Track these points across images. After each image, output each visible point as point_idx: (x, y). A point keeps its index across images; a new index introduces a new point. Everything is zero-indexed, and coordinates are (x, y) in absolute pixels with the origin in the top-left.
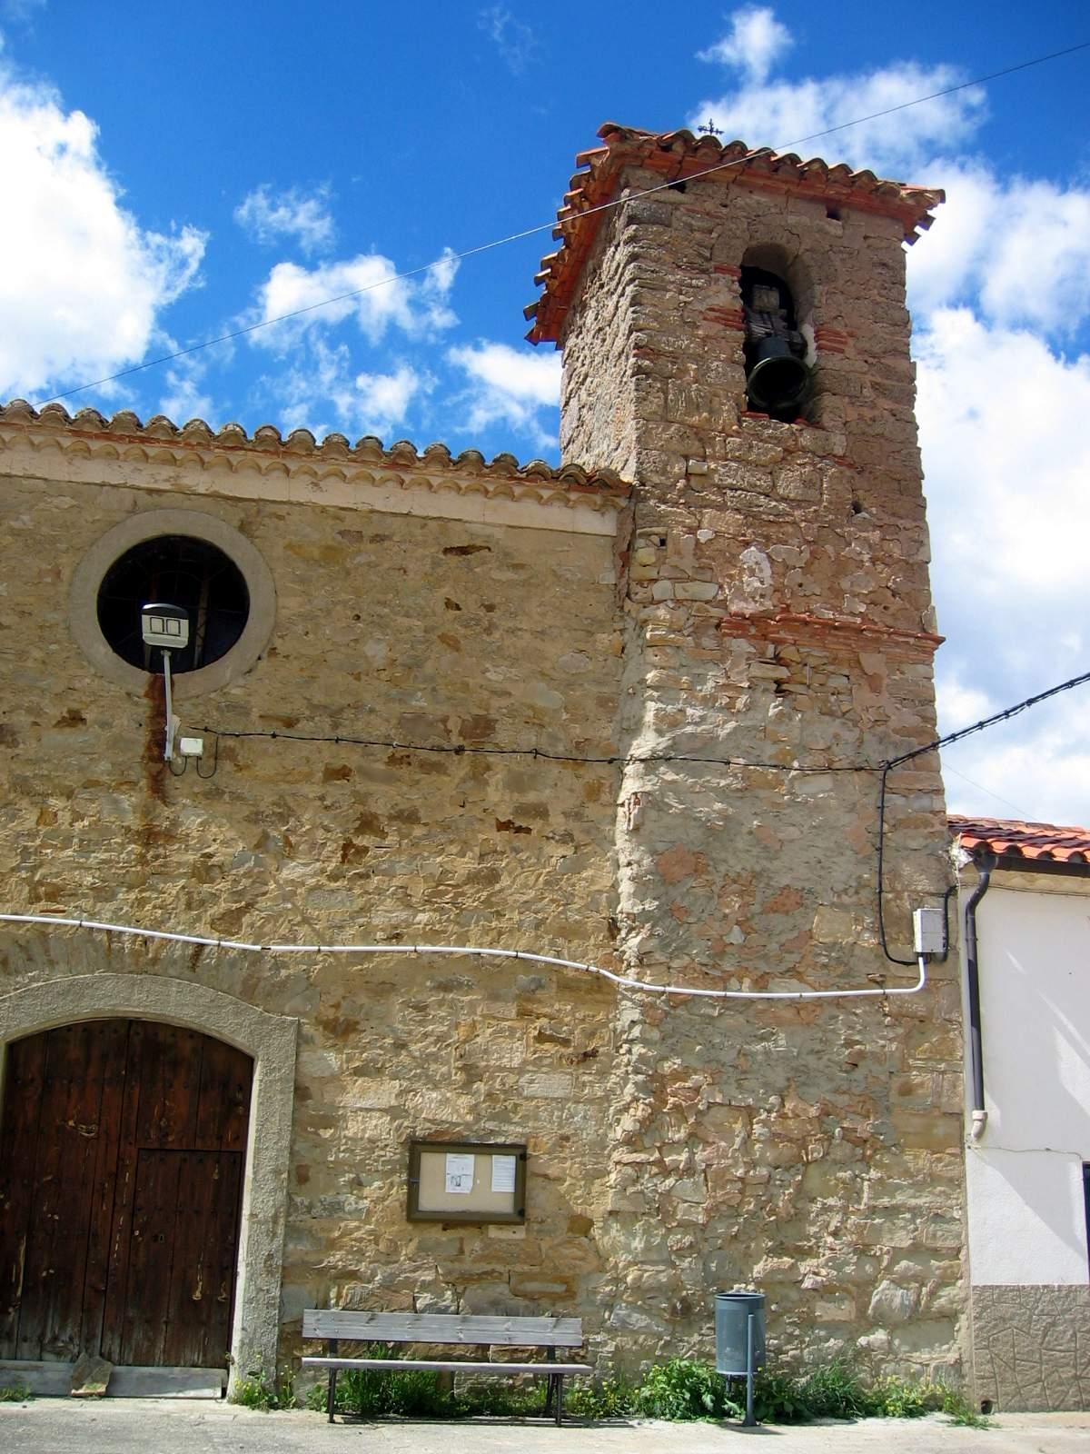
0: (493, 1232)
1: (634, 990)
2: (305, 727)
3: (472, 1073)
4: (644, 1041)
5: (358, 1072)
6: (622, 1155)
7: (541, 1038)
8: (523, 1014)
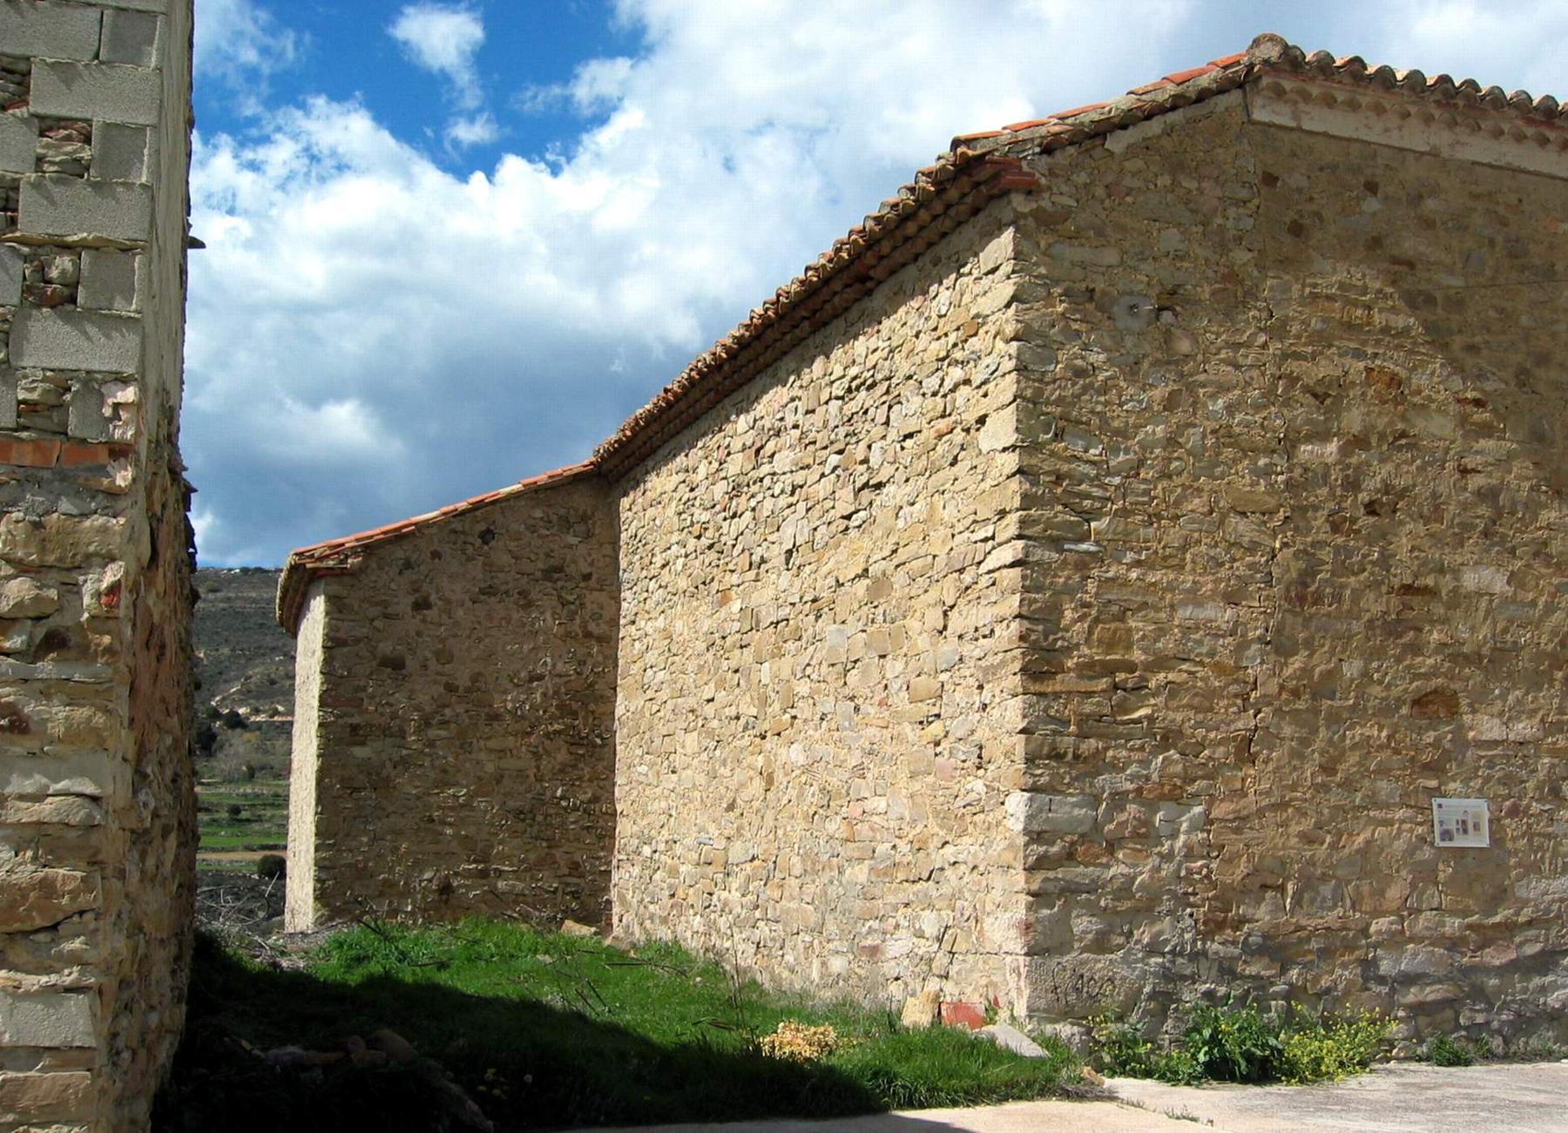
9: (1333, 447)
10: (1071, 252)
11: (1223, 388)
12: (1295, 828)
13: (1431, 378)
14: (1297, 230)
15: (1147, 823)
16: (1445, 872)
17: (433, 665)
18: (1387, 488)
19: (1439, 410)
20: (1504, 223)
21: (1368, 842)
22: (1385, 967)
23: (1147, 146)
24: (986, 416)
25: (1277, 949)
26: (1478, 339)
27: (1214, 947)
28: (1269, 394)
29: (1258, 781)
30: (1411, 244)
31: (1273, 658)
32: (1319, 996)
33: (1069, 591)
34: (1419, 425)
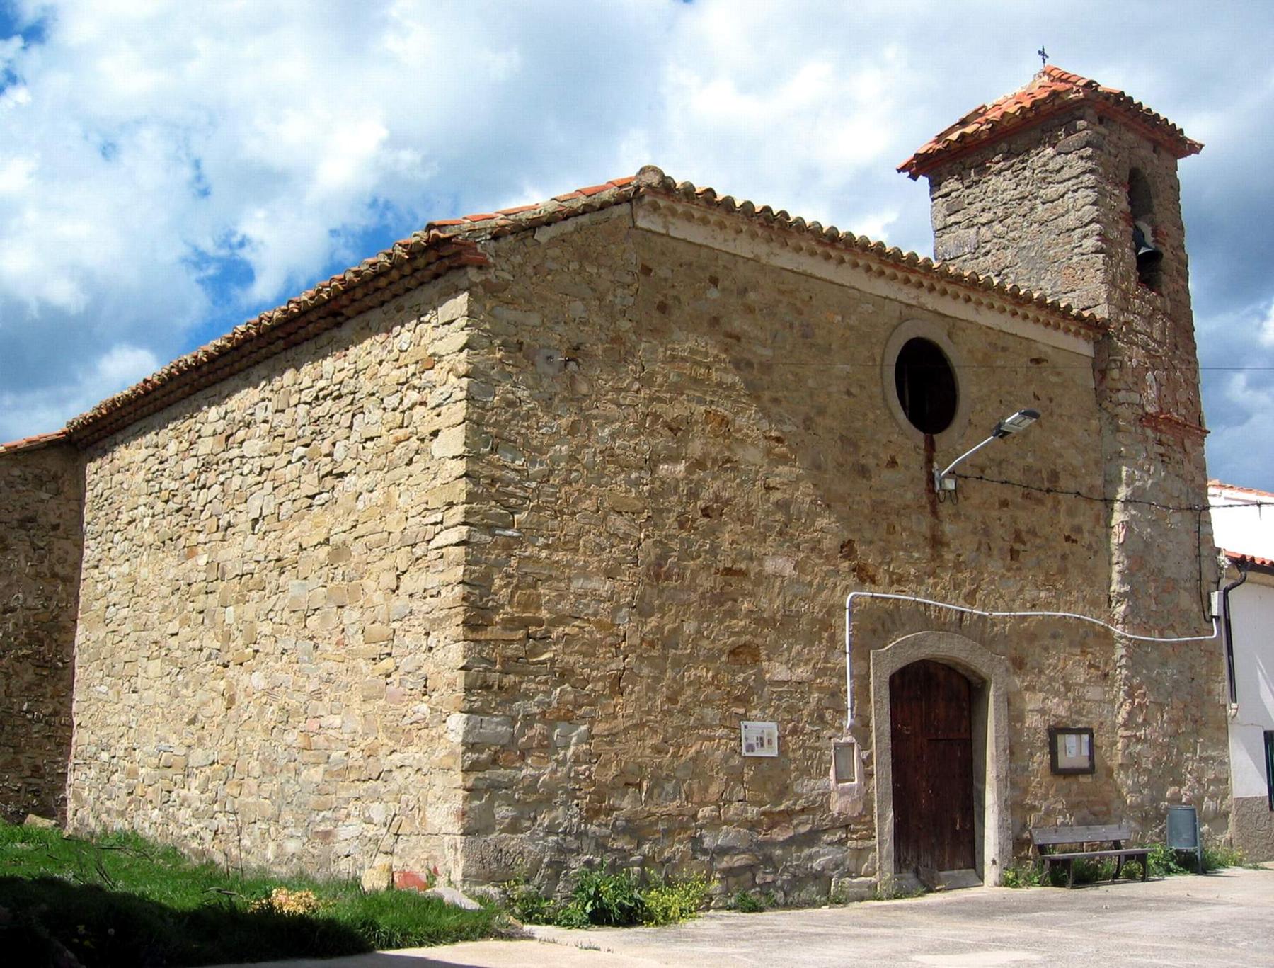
0: (1082, 779)
1: (1121, 637)
3: (1068, 686)
4: (1125, 666)
5: (1027, 688)
6: (1121, 732)
7: (1090, 666)
8: (1083, 652)
9: (681, 467)
10: (510, 314)
11: (608, 421)
12: (649, 742)
13: (748, 421)
14: (663, 308)
15: (548, 737)
16: (748, 774)
18: (717, 498)
19: (752, 443)
21: (698, 752)
22: (708, 842)
23: (563, 240)
24: (439, 430)
25: (635, 830)
26: (780, 394)
27: (592, 828)
28: (640, 427)
29: (625, 708)
30: (739, 324)
31: (636, 618)
32: (663, 863)
33: (498, 565)
34: (739, 454)
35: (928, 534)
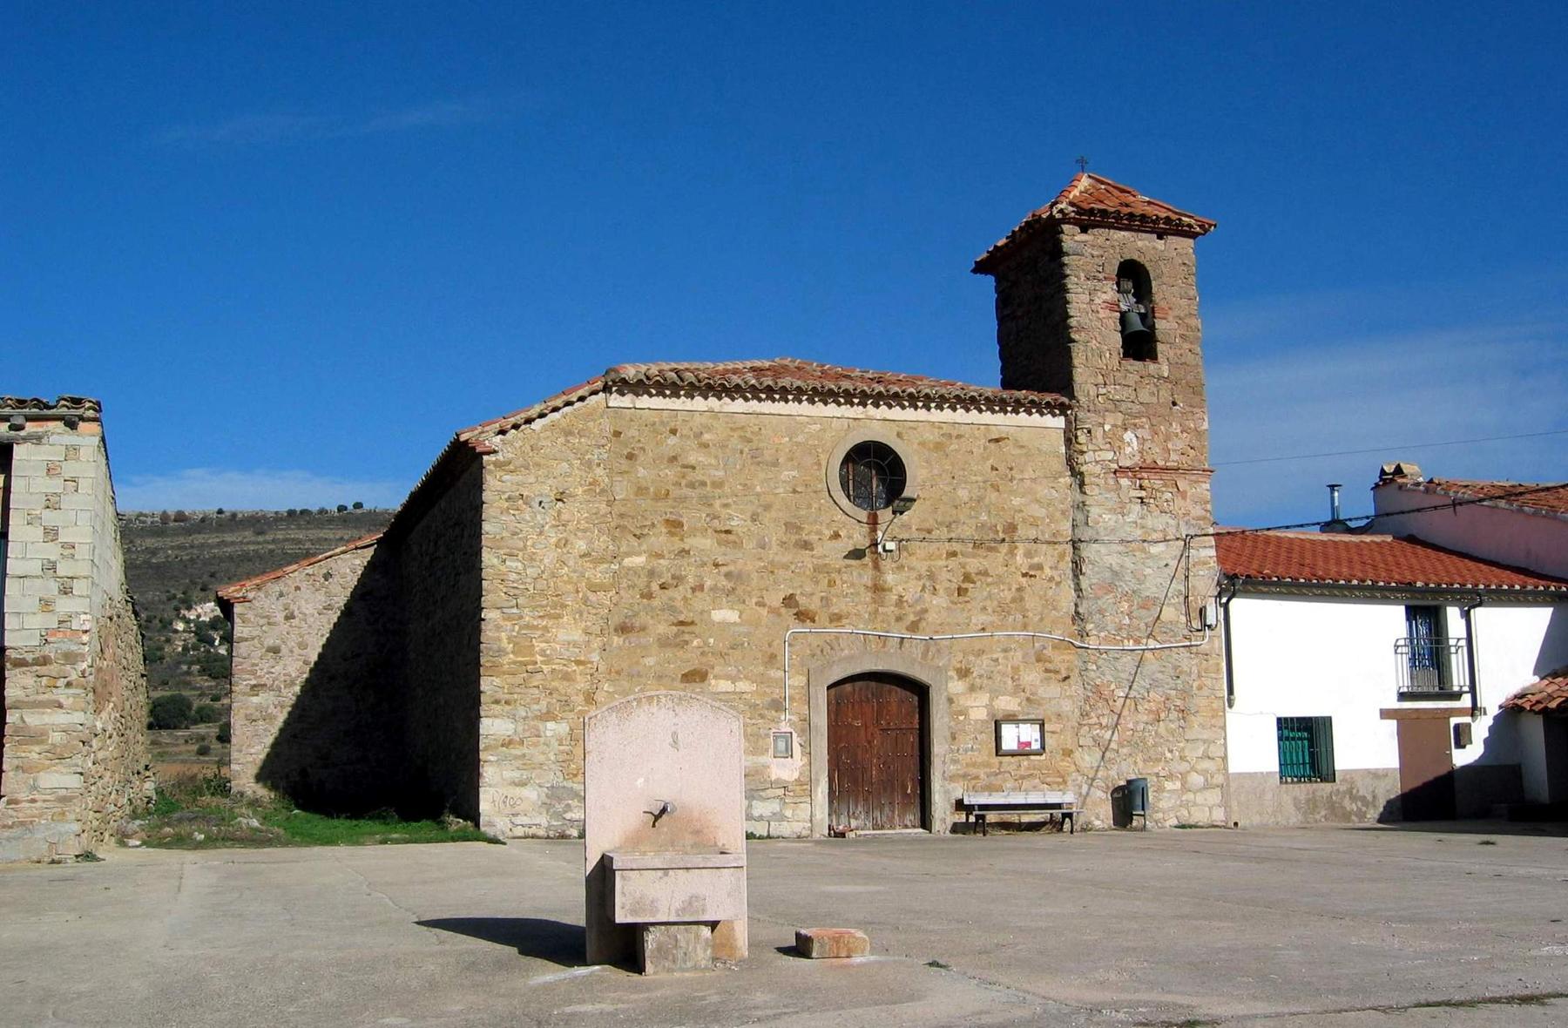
2: (936, 533)
14: (630, 457)
17: (296, 650)
20: (750, 441)
30: (692, 459)
35: (870, 584)
